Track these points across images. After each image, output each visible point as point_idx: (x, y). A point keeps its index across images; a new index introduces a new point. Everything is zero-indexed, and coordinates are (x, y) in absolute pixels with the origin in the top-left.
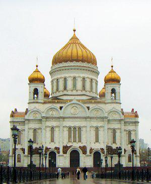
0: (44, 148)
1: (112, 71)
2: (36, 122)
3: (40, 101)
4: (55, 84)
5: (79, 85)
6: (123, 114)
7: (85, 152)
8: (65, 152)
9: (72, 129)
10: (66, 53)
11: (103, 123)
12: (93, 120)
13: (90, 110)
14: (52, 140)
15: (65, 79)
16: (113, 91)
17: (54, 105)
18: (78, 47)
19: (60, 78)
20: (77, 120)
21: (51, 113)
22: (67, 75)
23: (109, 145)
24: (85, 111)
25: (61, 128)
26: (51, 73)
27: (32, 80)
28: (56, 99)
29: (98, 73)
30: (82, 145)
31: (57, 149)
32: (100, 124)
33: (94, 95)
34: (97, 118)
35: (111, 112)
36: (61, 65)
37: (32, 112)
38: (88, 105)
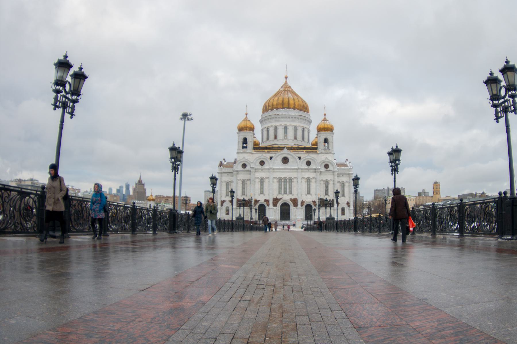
0: (253, 201)
3: (249, 151)
7: (296, 205)
8: (275, 205)
9: (283, 180)
10: (278, 100)
11: (315, 174)
13: (302, 160)
14: (262, 193)
16: (326, 141)
17: (264, 155)
20: (287, 171)
22: (278, 124)
23: (322, 197)
25: (271, 180)
26: (261, 122)
27: (241, 129)
29: (310, 122)
30: (293, 197)
31: (267, 201)
36: (270, 113)
38: (299, 156)
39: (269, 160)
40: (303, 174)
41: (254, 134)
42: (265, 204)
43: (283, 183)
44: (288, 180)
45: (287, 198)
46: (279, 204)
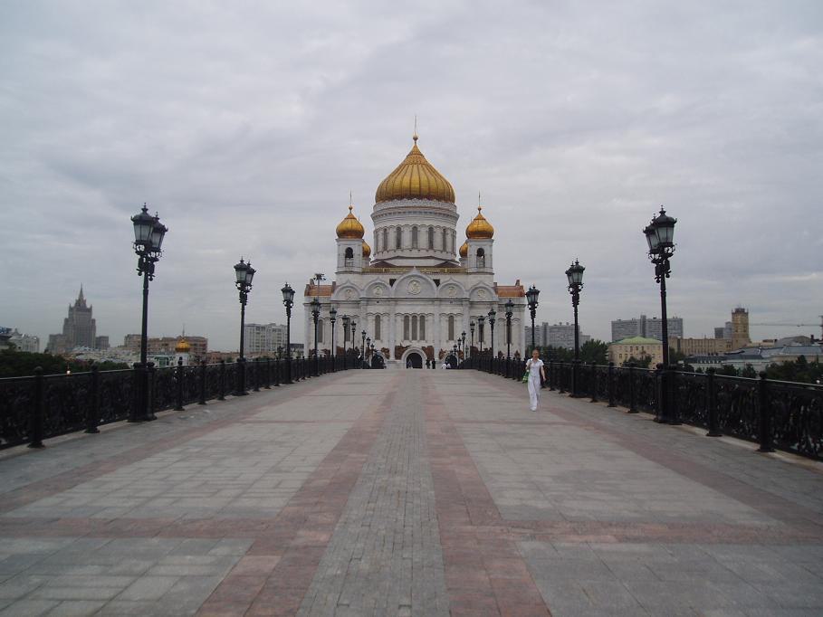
1: (480, 218)
2: (350, 305)
4: (381, 237)
5: (423, 239)
6: (496, 292)
8: (398, 356)
9: (411, 318)
10: (401, 182)
12: (443, 303)
13: (440, 287)
15: (399, 230)
16: (480, 253)
17: (381, 276)
18: (422, 172)
19: (391, 227)
20: (418, 303)
21: (375, 291)
22: (402, 223)
24: (432, 289)
25: (392, 316)
26: (375, 217)
28: (383, 266)
29: (456, 218)
31: (386, 351)
32: (456, 310)
33: (449, 257)
34: (451, 301)
35: (476, 288)
36: (391, 204)
37: (341, 290)
38: (436, 277)
39: (389, 286)
40: (443, 307)
41: (363, 242)
42: (383, 355)
43: (410, 323)
44: (418, 318)
45: (417, 345)
46: (405, 356)
